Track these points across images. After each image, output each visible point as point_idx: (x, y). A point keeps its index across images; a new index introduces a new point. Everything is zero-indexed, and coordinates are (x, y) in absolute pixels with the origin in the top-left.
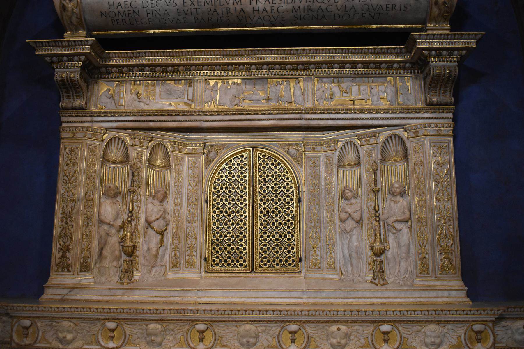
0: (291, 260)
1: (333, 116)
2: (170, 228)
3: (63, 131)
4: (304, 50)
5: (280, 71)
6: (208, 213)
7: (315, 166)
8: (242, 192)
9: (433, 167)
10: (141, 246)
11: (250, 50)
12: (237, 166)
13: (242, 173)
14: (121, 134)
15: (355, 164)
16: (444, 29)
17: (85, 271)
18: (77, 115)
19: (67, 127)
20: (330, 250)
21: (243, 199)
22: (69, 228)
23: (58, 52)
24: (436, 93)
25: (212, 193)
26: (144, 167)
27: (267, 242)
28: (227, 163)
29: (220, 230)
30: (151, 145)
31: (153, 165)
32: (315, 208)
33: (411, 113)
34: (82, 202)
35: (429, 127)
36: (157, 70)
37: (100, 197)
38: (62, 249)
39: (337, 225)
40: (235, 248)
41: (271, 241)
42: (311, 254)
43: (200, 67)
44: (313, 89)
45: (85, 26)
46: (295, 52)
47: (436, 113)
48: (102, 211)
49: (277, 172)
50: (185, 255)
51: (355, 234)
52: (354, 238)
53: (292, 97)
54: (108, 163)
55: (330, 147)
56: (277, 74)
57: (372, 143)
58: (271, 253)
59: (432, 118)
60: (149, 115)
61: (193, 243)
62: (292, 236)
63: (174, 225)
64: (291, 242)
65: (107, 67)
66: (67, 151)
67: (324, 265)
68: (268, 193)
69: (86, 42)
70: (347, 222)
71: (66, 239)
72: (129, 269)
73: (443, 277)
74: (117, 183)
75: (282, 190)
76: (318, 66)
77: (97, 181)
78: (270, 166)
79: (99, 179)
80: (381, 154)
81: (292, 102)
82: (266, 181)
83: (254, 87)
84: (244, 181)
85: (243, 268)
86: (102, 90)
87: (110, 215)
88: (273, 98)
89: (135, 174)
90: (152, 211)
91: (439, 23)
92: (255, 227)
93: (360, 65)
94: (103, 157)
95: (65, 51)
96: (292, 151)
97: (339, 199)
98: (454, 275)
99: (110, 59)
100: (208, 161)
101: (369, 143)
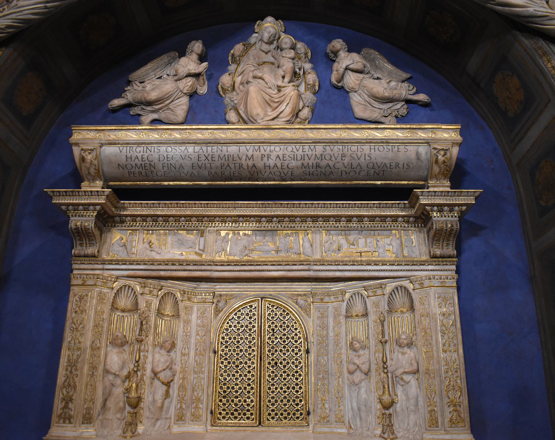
0: (299, 413)
1: (340, 268)
2: (176, 378)
3: (74, 277)
4: (312, 204)
5: (323, 224)
6: (216, 364)
7: (323, 316)
8: (250, 342)
9: (439, 318)
10: (146, 397)
11: (261, 203)
12: (246, 317)
13: (250, 323)
14: (131, 282)
15: (363, 315)
16: (444, 186)
17: (87, 423)
18: (89, 262)
19: (78, 274)
20: (339, 403)
21: (251, 350)
22: (73, 377)
23: (74, 202)
24: (439, 246)
25: (220, 343)
26: (152, 316)
27: (275, 394)
28: (236, 313)
29: (228, 382)
30: (161, 294)
31: (162, 314)
32: (324, 359)
33: (416, 265)
34: (88, 351)
35: (434, 279)
36: (169, 221)
37: (107, 345)
38: (64, 400)
39: (346, 377)
40: (242, 400)
41: (279, 393)
42: (319, 407)
43: (212, 218)
44: (321, 242)
45: (102, 177)
46: (304, 206)
47: (440, 265)
48: (108, 361)
49: (285, 322)
50: (191, 407)
51: (363, 387)
52: (363, 391)
53: (301, 248)
54: (117, 311)
55: (338, 298)
56: (286, 226)
57: (379, 294)
58: (279, 406)
59: (436, 270)
60: (160, 264)
61: (200, 395)
62: (300, 388)
63: (181, 376)
64: (299, 395)
65: (120, 216)
66: (77, 298)
67: (333, 419)
68: (276, 344)
69: (102, 193)
70: (355, 374)
71: (70, 389)
72: (133, 421)
73: (452, 430)
74: (125, 331)
75: (290, 341)
76: (326, 220)
77: (105, 329)
78: (278, 317)
79: (107, 327)
80: (388, 306)
81: (301, 254)
82: (275, 331)
83: (264, 239)
84: (252, 331)
85: (250, 422)
86: (115, 238)
87: (116, 364)
88: (283, 249)
89: (143, 323)
90: (158, 361)
91: (440, 180)
92: (263, 379)
93: (366, 219)
94: (112, 305)
95: (82, 200)
96: (301, 301)
97: (347, 350)
98: (463, 428)
99: (125, 209)
100: (218, 311)
101: (376, 295)
